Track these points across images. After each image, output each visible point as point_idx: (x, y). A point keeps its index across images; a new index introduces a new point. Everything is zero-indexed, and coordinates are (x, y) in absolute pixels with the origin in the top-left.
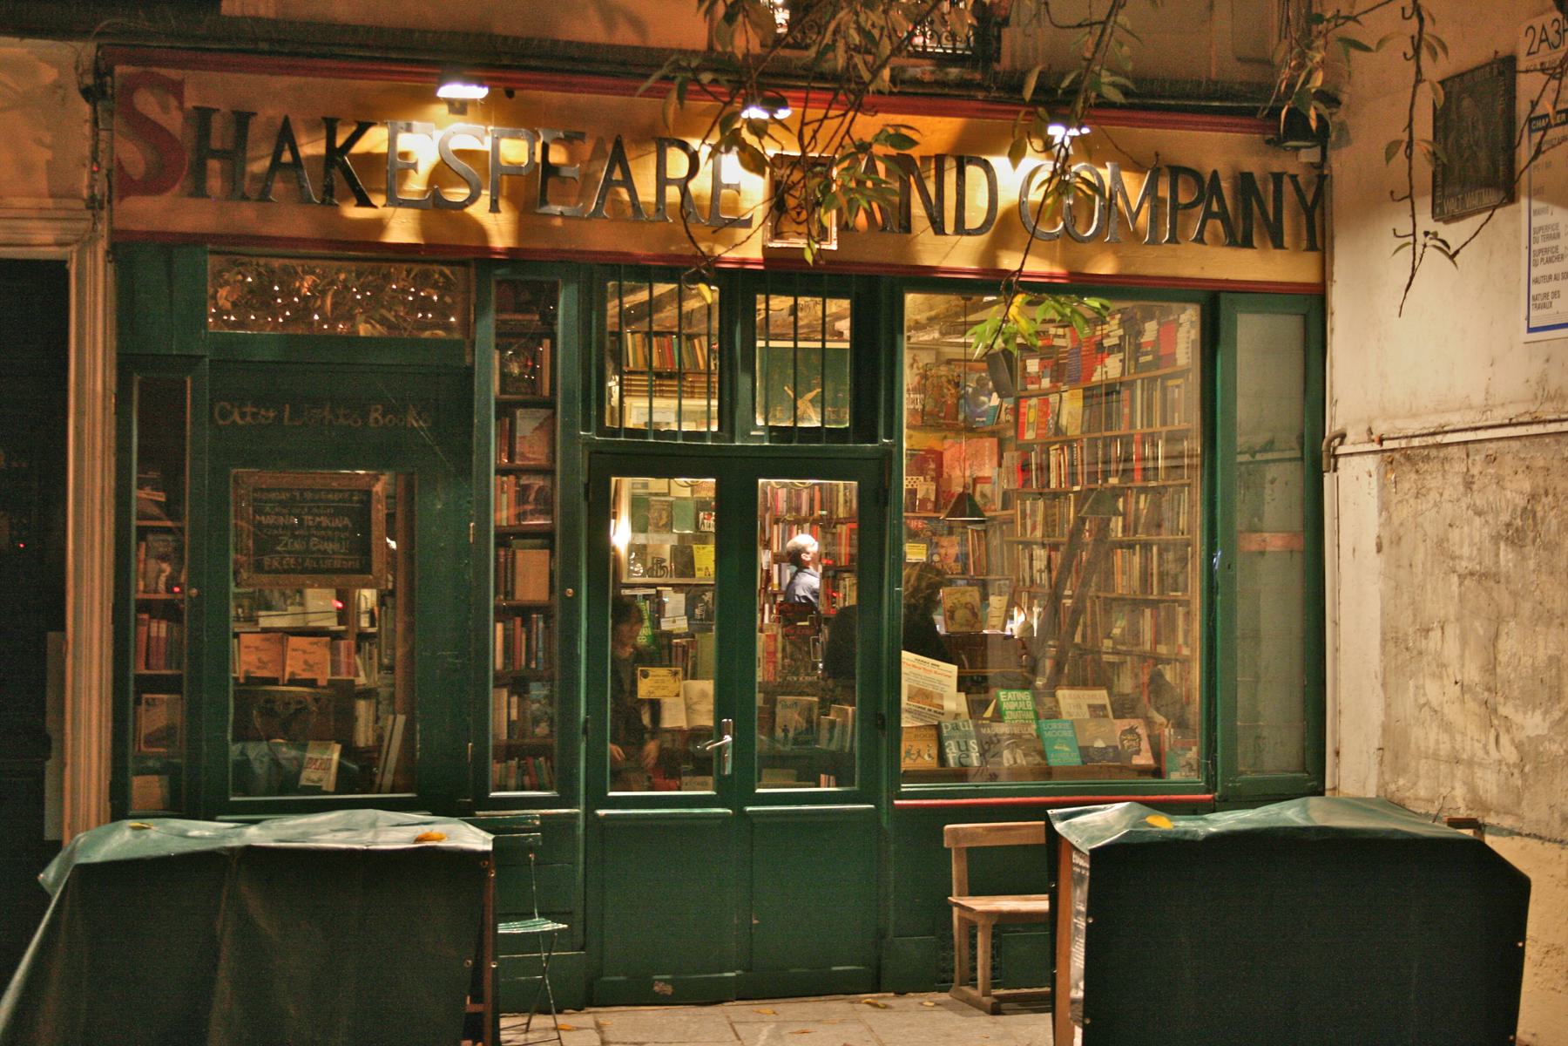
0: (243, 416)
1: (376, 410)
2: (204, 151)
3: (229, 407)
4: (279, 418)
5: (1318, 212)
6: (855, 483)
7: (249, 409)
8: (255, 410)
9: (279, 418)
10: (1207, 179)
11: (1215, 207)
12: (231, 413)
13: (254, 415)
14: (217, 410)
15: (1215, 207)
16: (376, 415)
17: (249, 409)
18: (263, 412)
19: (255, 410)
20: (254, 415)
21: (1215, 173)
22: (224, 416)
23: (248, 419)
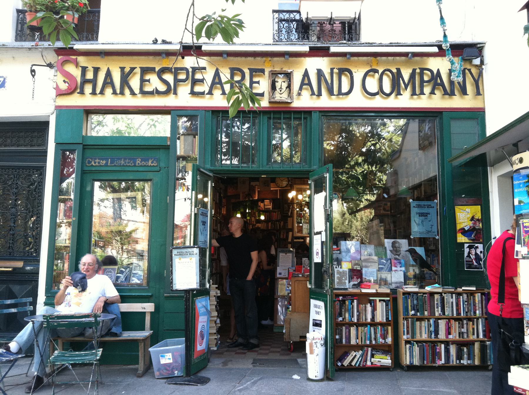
0: (95, 163)
1: (139, 160)
2: (85, 81)
3: (91, 160)
4: (107, 163)
5: (480, 82)
9: (107, 163)
10: (435, 72)
11: (439, 81)
12: (91, 162)
13: (99, 163)
15: (439, 81)
17: (97, 161)
18: (101, 161)
20: (99, 163)
21: (438, 70)
22: (89, 162)
23: (97, 164)
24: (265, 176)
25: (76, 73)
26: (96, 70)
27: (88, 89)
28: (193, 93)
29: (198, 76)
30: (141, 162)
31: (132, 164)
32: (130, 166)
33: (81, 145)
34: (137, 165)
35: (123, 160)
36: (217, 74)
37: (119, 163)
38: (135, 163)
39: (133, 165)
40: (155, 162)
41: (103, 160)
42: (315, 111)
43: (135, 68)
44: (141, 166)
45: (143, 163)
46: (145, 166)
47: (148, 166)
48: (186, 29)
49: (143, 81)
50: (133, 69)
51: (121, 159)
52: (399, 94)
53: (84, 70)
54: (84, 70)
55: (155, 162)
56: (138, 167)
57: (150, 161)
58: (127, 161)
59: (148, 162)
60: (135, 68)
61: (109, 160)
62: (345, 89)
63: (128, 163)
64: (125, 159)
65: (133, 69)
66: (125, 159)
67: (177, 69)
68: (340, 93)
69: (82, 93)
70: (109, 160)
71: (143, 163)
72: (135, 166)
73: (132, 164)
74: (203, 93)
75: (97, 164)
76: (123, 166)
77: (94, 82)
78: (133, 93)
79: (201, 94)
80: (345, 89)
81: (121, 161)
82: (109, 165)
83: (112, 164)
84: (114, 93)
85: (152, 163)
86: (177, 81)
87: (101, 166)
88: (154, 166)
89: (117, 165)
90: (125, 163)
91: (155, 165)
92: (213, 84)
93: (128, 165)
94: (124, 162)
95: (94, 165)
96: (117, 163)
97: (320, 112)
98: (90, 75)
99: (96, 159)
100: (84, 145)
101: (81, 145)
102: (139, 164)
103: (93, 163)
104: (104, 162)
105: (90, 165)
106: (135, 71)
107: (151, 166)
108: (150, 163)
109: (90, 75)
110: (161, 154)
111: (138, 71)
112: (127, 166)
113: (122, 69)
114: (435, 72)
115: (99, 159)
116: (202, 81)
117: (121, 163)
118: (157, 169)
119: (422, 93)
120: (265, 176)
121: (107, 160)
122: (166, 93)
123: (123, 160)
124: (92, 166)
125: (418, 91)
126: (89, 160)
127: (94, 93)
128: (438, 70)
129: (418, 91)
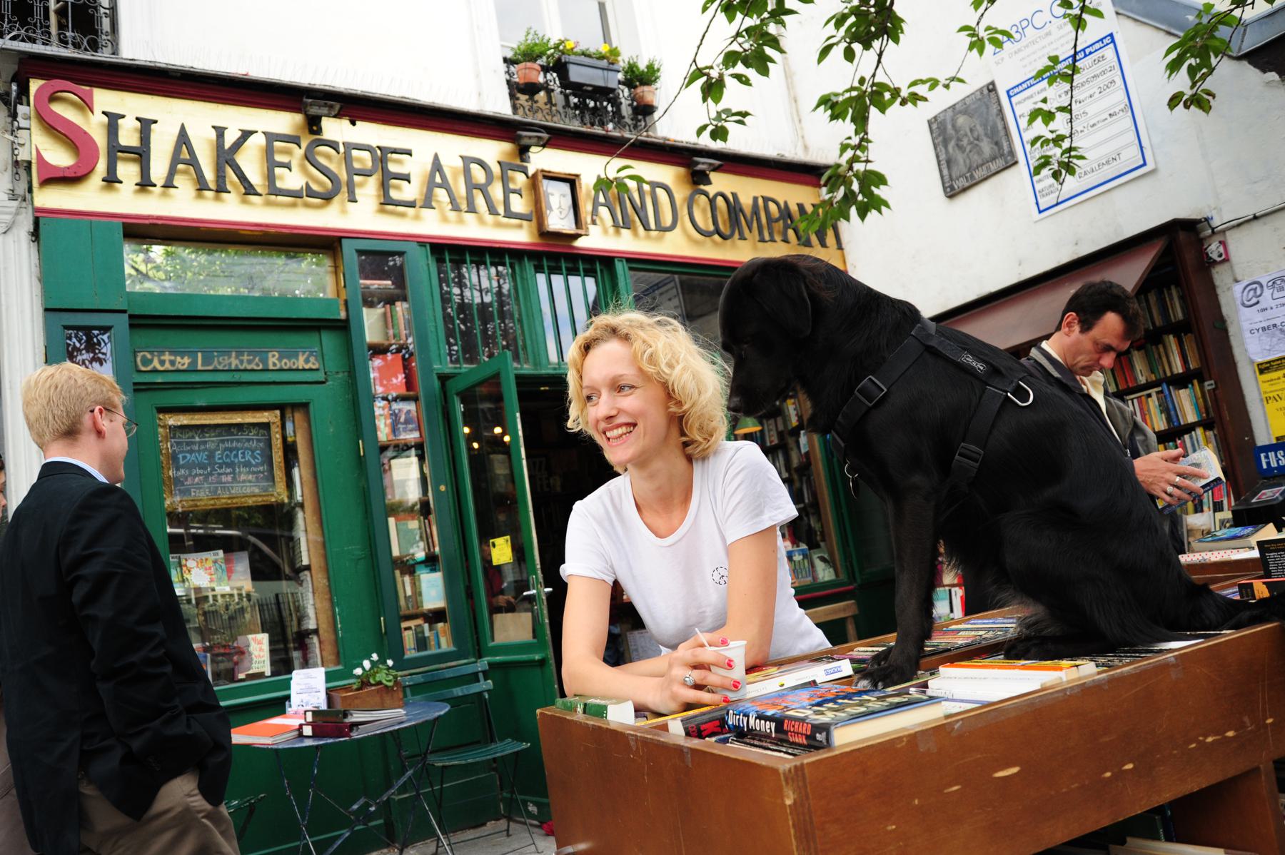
0: (162, 362)
1: (274, 356)
2: (116, 151)
3: (149, 356)
4: (194, 362)
6: (508, 537)
7: (167, 357)
8: (173, 358)
10: (782, 205)
12: (151, 361)
13: (172, 363)
14: (139, 359)
16: (274, 360)
17: (167, 357)
18: (179, 359)
19: (173, 358)
20: (172, 363)
22: (146, 362)
24: (547, 388)
25: (94, 126)
26: (146, 126)
27: (128, 172)
28: (387, 202)
29: (393, 168)
30: (280, 359)
31: (258, 365)
32: (253, 370)
33: (126, 316)
34: (271, 367)
35: (234, 354)
36: (437, 166)
37: (227, 362)
38: (265, 361)
39: (261, 367)
40: (312, 359)
41: (182, 354)
42: (621, 259)
43: (251, 133)
44: (281, 370)
45: (286, 364)
46: (290, 370)
47: (297, 370)
48: (694, 61)
49: (271, 165)
50: (246, 134)
51: (228, 354)
52: (742, 238)
53: (113, 120)
54: (113, 120)
55: (312, 359)
56: (274, 373)
57: (301, 359)
58: (245, 358)
59: (297, 359)
60: (251, 133)
61: (200, 354)
62: (667, 219)
63: (249, 362)
64: (239, 354)
65: (246, 134)
66: (239, 354)
67: (350, 146)
68: (662, 229)
69: (111, 180)
70: (200, 354)
71: (286, 364)
72: (266, 370)
73: (258, 365)
74: (411, 205)
75: (167, 366)
76: (237, 370)
77: (141, 155)
78: (249, 190)
79: (411, 205)
80: (667, 219)
81: (230, 357)
82: (200, 367)
83: (210, 364)
84: (202, 186)
85: (307, 361)
86: (352, 172)
87: (178, 371)
88: (311, 370)
89: (220, 368)
90: (242, 362)
91: (314, 367)
92: (431, 185)
93: (249, 367)
94: (237, 362)
95: (160, 368)
96: (220, 363)
97: (629, 260)
98: (128, 136)
99: (162, 353)
100: (131, 317)
101: (126, 316)
102: (274, 364)
103: (156, 364)
104: (186, 360)
105: (149, 368)
106: (252, 139)
107: (304, 370)
108: (301, 363)
109: (128, 136)
110: (329, 340)
111: (257, 141)
112: (245, 370)
113: (220, 131)
114: (782, 205)
115: (172, 353)
116: (407, 178)
117: (230, 364)
118: (320, 376)
119: (773, 240)
120: (547, 388)
121: (192, 355)
122: (327, 198)
123: (234, 354)
124: (155, 371)
125: (767, 237)
126: (144, 357)
127: (145, 184)
128: (786, 203)
129: (767, 237)
